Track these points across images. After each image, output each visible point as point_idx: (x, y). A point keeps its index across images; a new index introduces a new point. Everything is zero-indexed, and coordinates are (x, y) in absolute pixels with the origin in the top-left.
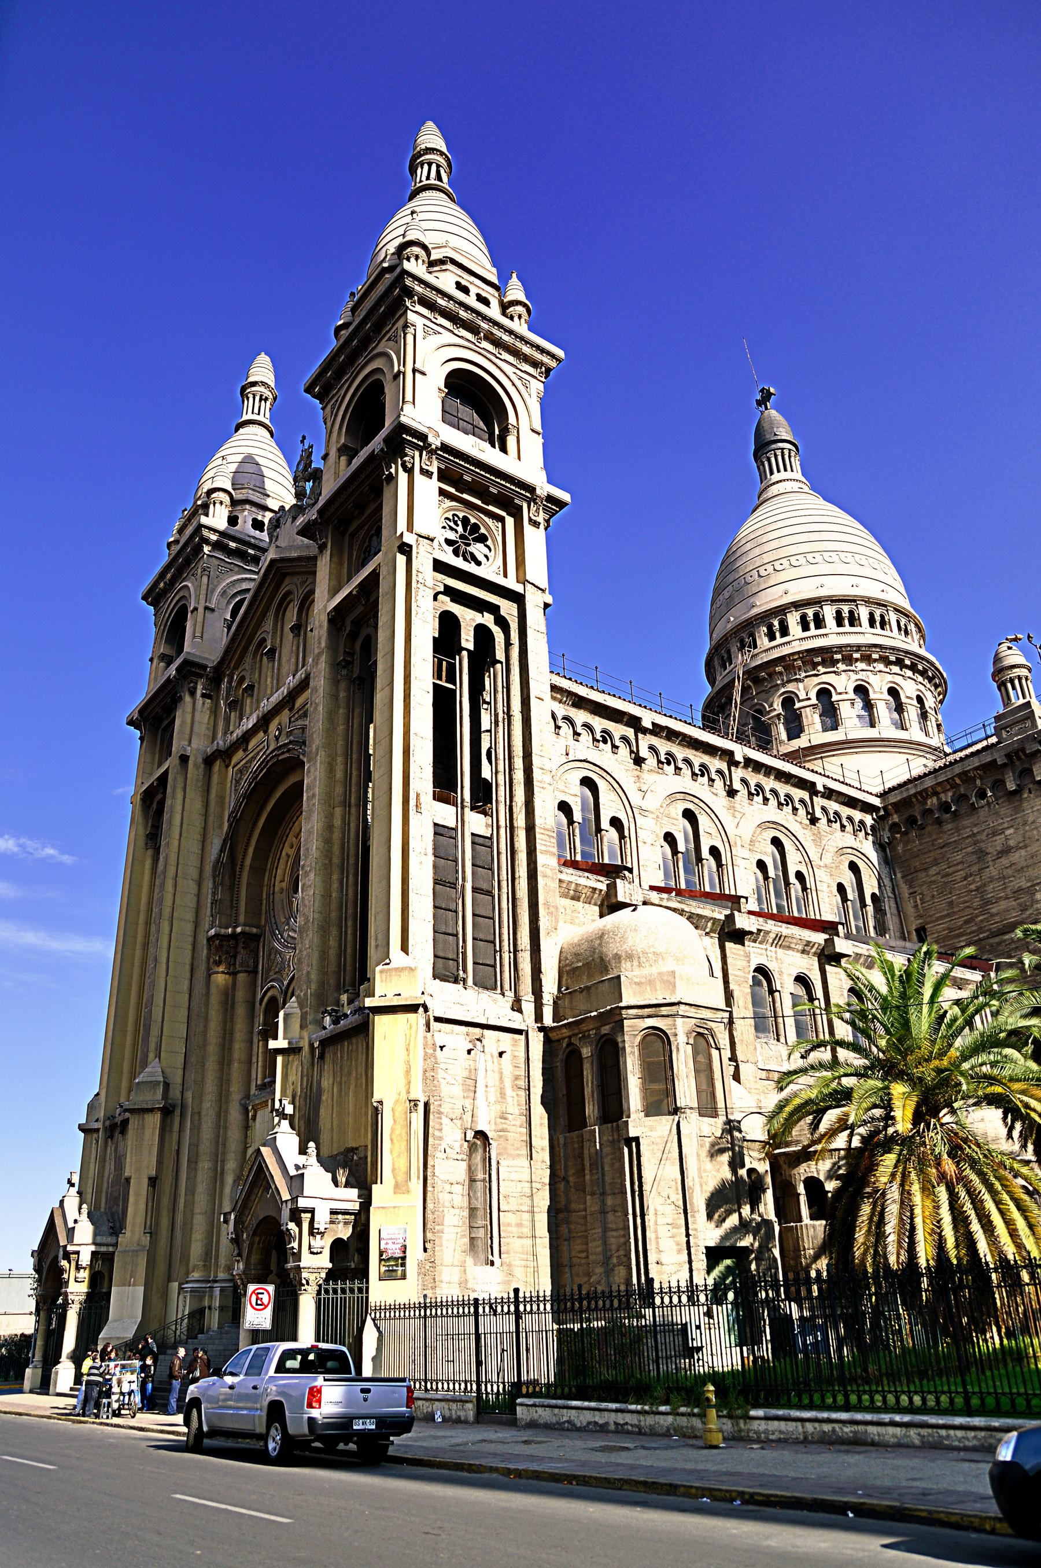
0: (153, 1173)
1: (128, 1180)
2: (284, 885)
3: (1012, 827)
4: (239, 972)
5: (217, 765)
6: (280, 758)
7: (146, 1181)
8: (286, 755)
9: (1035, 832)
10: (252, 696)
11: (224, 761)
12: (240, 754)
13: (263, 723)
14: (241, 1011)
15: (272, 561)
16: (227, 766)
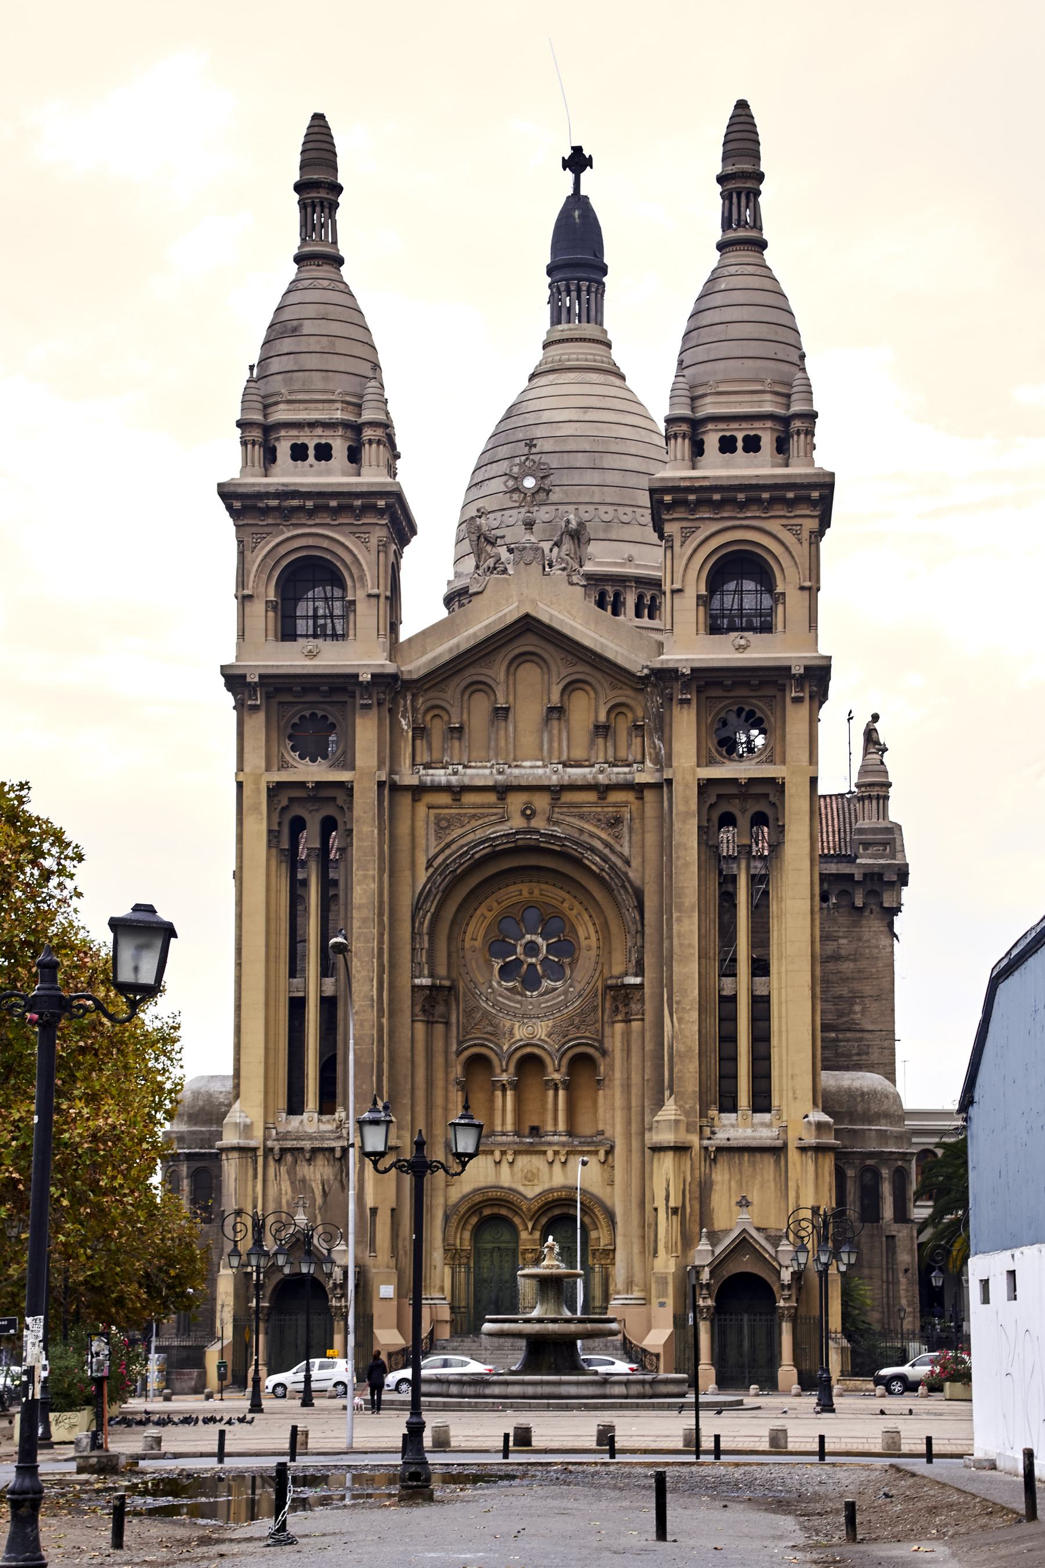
0: (394, 1205)
1: (374, 1211)
2: (478, 944)
3: (846, 937)
4: (437, 1022)
5: (406, 800)
6: (542, 845)
7: (389, 1212)
8: (558, 848)
9: (867, 951)
10: (460, 739)
11: (413, 795)
12: (445, 799)
13: (503, 791)
14: (439, 1060)
15: (527, 616)
16: (419, 800)
